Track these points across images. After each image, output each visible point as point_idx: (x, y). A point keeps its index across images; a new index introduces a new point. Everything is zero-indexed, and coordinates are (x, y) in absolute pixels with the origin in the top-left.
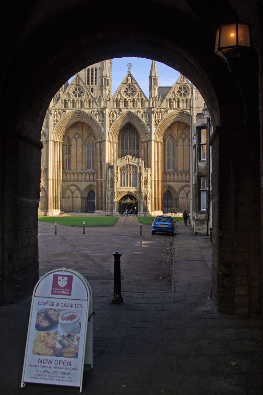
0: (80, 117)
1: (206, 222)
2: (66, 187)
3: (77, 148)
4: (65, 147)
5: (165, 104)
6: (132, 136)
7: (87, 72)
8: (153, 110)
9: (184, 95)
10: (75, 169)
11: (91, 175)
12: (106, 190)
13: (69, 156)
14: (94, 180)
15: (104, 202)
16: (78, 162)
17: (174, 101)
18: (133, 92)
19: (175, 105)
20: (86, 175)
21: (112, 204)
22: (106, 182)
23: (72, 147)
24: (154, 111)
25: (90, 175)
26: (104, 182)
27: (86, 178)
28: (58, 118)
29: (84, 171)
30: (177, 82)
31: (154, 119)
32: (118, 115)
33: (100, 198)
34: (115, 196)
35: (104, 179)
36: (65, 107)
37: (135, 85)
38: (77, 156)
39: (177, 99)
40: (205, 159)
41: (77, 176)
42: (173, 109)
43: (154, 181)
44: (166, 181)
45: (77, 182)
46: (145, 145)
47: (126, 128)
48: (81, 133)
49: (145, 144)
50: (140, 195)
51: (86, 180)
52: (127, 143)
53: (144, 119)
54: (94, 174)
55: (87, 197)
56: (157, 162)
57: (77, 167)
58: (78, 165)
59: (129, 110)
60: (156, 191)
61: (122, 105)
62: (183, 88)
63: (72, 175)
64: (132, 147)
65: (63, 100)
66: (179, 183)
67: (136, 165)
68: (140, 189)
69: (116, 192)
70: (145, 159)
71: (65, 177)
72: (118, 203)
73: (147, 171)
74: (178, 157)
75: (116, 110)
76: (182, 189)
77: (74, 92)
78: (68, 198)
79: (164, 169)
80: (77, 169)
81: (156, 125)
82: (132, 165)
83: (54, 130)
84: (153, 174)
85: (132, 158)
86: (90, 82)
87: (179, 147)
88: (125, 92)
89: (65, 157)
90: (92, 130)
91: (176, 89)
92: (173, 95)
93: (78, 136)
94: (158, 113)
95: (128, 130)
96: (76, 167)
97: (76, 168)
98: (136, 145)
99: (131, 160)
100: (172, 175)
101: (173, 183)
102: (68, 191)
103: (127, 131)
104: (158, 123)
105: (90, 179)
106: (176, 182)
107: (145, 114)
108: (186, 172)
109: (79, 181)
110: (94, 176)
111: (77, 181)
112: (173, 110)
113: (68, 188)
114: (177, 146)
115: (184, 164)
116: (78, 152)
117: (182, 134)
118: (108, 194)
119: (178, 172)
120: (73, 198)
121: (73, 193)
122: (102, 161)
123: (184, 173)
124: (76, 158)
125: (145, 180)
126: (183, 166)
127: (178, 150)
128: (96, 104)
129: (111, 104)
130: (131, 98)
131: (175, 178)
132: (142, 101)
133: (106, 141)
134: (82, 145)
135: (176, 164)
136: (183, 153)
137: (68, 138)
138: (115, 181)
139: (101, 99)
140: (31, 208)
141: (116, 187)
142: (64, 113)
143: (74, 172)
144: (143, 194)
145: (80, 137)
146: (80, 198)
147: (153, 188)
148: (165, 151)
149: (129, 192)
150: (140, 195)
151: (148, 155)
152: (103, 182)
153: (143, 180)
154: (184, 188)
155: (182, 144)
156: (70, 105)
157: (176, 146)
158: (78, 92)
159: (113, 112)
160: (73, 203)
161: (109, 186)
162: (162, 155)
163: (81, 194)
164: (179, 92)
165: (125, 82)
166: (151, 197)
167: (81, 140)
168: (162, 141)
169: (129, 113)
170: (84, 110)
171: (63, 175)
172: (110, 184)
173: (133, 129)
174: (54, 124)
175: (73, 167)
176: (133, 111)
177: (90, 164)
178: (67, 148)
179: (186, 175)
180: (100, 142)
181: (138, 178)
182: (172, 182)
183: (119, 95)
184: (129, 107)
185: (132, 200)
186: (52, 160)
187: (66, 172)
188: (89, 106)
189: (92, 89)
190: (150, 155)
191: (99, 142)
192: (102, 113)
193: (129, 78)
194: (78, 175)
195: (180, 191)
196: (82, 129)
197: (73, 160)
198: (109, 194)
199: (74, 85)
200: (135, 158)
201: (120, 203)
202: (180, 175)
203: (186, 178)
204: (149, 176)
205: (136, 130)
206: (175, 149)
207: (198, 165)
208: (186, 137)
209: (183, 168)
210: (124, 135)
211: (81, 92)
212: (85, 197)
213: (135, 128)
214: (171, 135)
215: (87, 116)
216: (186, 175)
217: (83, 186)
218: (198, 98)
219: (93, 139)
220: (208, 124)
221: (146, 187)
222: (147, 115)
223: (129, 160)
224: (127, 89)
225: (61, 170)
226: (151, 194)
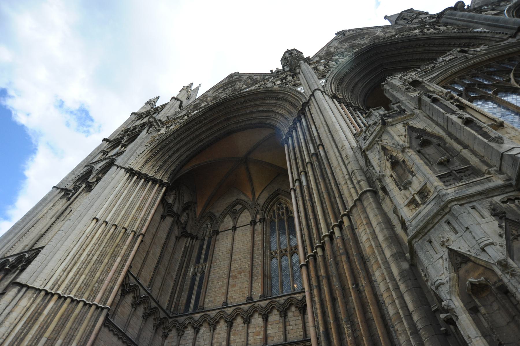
11: (290, 314)
16: (235, 277)
20: (266, 319)
25: (284, 314)
27: (266, 337)
41: (225, 335)
48: (251, 197)
54: (303, 309)
58: (235, 286)
105: (285, 335)
116: (236, 246)
167: (248, 214)
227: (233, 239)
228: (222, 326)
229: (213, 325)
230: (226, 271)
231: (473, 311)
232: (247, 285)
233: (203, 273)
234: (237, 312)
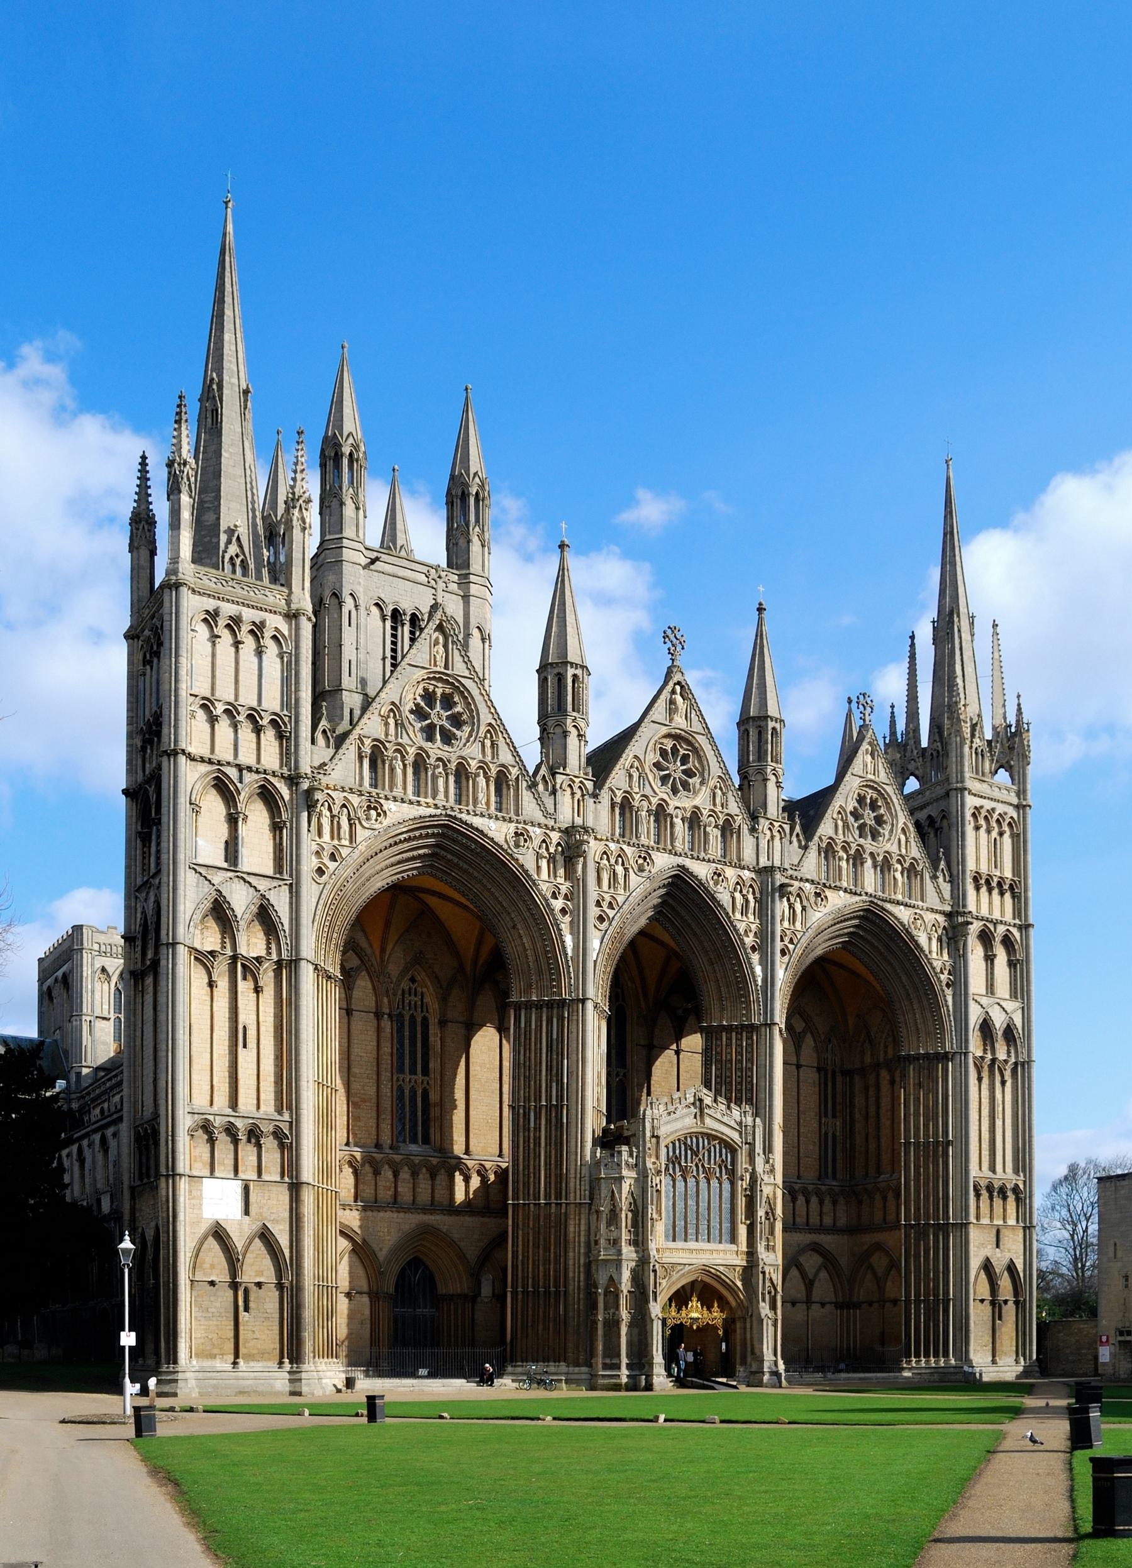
5: (812, 864)
7: (389, 623)
8: (779, 879)
9: (875, 835)
18: (689, 773)
24: (782, 886)
28: (339, 839)
29: (388, 1151)
42: (845, 891)
46: (729, 1045)
49: (729, 1039)
53: (738, 916)
59: (680, 860)
62: (868, 801)
65: (368, 742)
68: (751, 1254)
75: (625, 847)
82: (715, 1138)
83: (321, 902)
88: (657, 765)
91: (849, 799)
94: (792, 899)
104: (791, 947)
107: (745, 892)
112: (841, 893)
115: (802, 1151)
118: (611, 1279)
122: (559, 1108)
128: (538, 799)
132: (727, 829)
139: (559, 779)
149: (706, 1270)
152: (566, 1213)
153: (761, 1213)
156: (404, 778)
159: (613, 861)
164: (856, 815)
174: (320, 871)
176: (701, 870)
180: (550, 1005)
181: (741, 1202)
183: (636, 775)
184: (678, 845)
185: (709, 1308)
191: (539, 1006)
192: (570, 851)
216: (808, 1202)
222: (750, 897)
223: (701, 1110)
224: (663, 753)
231: (605, 1295)
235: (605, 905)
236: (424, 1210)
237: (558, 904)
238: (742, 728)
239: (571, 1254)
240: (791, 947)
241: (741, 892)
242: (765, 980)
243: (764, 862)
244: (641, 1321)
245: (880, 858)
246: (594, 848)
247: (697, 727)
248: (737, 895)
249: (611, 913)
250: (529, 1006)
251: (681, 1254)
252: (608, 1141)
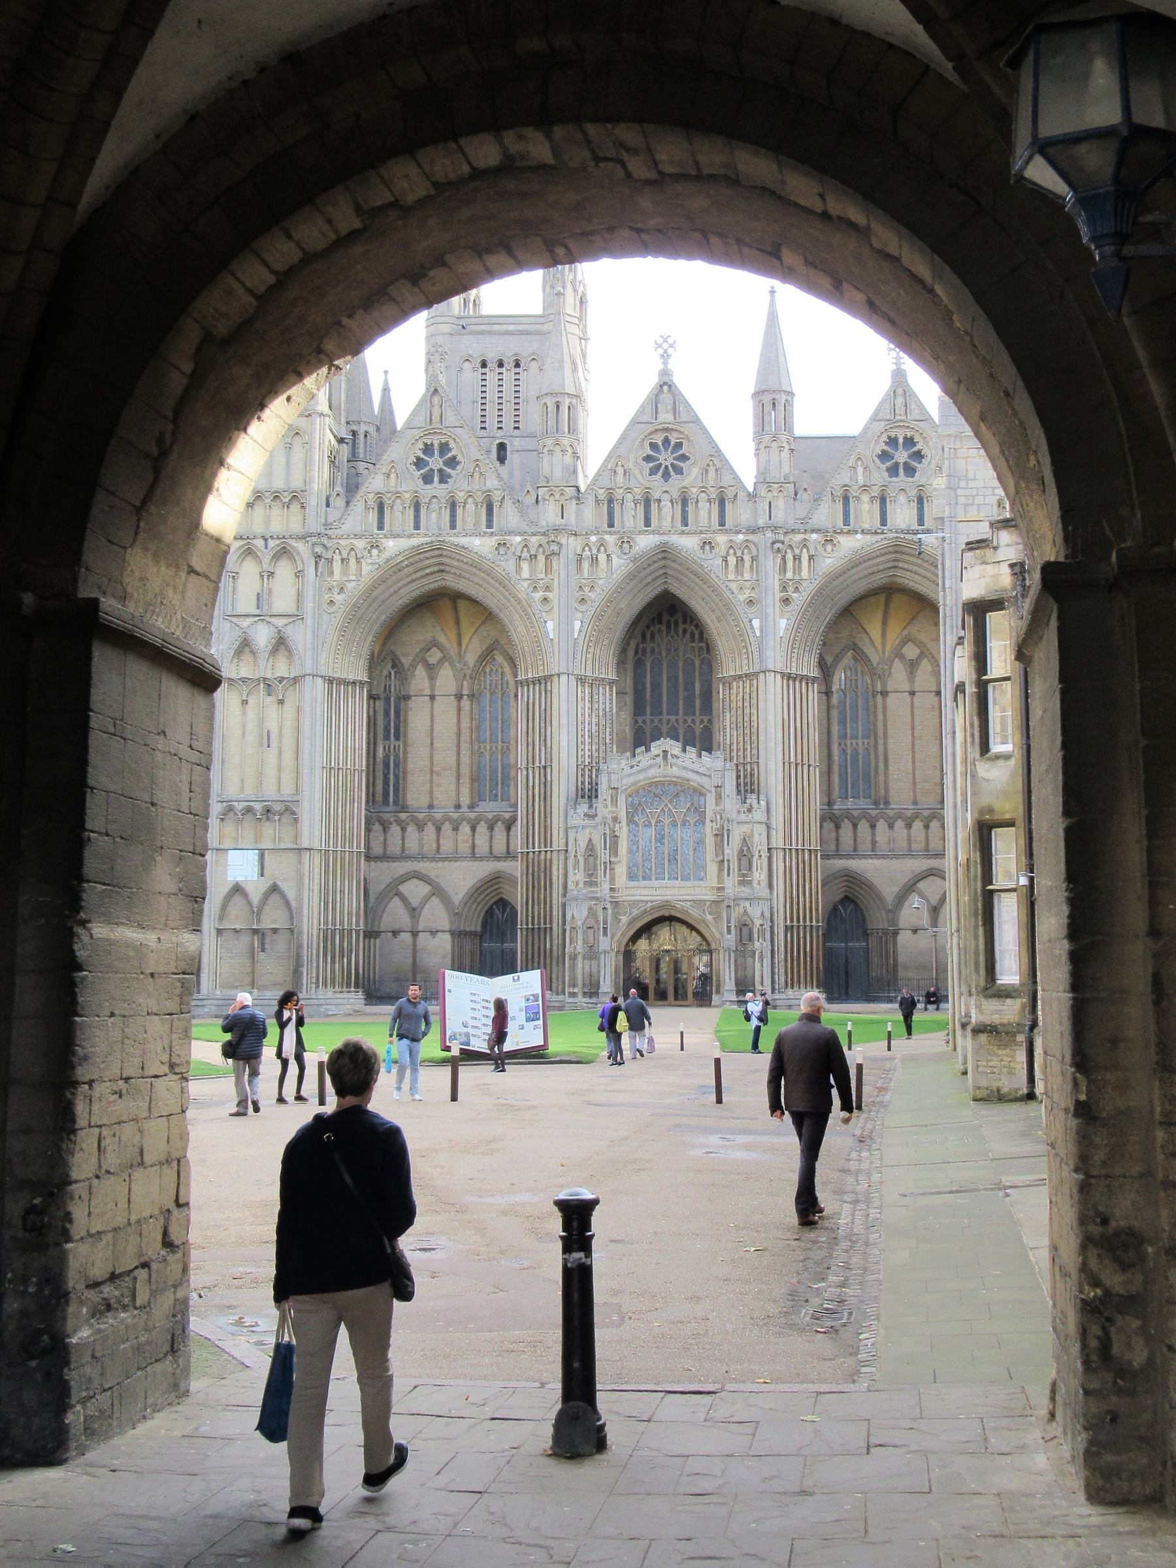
0: (449, 572)
1: (1021, 1038)
2: (382, 887)
3: (436, 708)
4: (380, 705)
5: (827, 514)
6: (681, 654)
10: (426, 804)
11: (496, 829)
12: (564, 895)
13: (397, 743)
14: (509, 855)
15: (555, 954)
16: (438, 774)
17: (865, 498)
18: (684, 458)
19: (866, 512)
20: (473, 829)
21: (594, 963)
22: (566, 859)
23: (411, 704)
25: (491, 828)
26: (555, 862)
27: (473, 847)
30: (876, 413)
31: (777, 577)
32: (616, 561)
33: (539, 932)
34: (605, 922)
35: (555, 847)
36: (380, 528)
37: (687, 429)
38: (432, 744)
39: (875, 491)
40: (1008, 748)
41: (433, 837)
43: (781, 854)
44: (837, 854)
45: (433, 864)
46: (737, 694)
47: (653, 620)
50: (717, 918)
51: (473, 853)
52: (656, 686)
53: (731, 576)
54: (509, 825)
55: (479, 929)
56: (793, 766)
57: (436, 794)
58: (440, 785)
59: (666, 538)
60: (792, 898)
61: (630, 517)
62: (901, 441)
63: (411, 829)
64: (681, 702)
66: (894, 862)
67: (704, 781)
69: (609, 906)
70: (741, 753)
71: (382, 838)
72: (621, 958)
73: (749, 810)
74: (890, 746)
76: (910, 888)
77: (419, 463)
78: (395, 933)
79: (826, 800)
80: (435, 803)
81: (786, 601)
84: (778, 820)
85: (684, 750)
86: (492, 423)
87: (891, 699)
88: (648, 459)
89: (381, 750)
90: (503, 630)
92: (860, 470)
93: (439, 655)
95: (664, 628)
96: (431, 792)
97: (432, 798)
98: (697, 692)
99: (679, 762)
100: (864, 827)
101: (870, 861)
102: (391, 905)
103: (660, 631)
105: (491, 847)
106: (885, 857)
107: (739, 554)
108: (926, 813)
109: (445, 859)
110: (511, 833)
111: (433, 859)
113: (394, 889)
114: (884, 694)
115: (917, 776)
116: (437, 728)
117: (904, 643)
119: (891, 813)
120: (415, 934)
121: (417, 912)
122: (545, 767)
123: (916, 816)
124: (432, 756)
125: (741, 850)
126: (914, 784)
127: (889, 714)
129: (591, 515)
130: (676, 482)
131: (877, 839)
133: (564, 678)
134: (459, 697)
135: (881, 778)
136: (913, 728)
137: (393, 667)
138: (603, 855)
139: (541, 492)
140: (152, 975)
141: (612, 880)
142: (375, 552)
143: (420, 816)
144: (734, 915)
145: (446, 658)
146: (447, 937)
147: (779, 884)
148: (829, 719)
149: (666, 904)
150: (717, 918)
151: (754, 738)
154: (920, 885)
155: (907, 687)
157: (879, 697)
158: (436, 463)
160: (414, 958)
161: (577, 876)
162: (815, 736)
163: (455, 915)
164: (884, 456)
165: (646, 418)
166: (772, 927)
168: (814, 672)
169: (664, 553)
170: (464, 541)
171: (368, 830)
172: (582, 868)
173: (685, 622)
175: (416, 796)
176: (688, 543)
177: (490, 779)
178: (387, 713)
179: (927, 827)
181: (710, 841)
182: (864, 857)
183: (620, 470)
186: (318, 766)
187: (386, 816)
188: (490, 526)
189: (502, 447)
190: (761, 738)
193: (666, 397)
194: (438, 829)
195: (902, 898)
196: (458, 623)
197: (417, 760)
198: (578, 913)
199: (417, 433)
200: (693, 750)
201: (628, 956)
202: (899, 824)
203: (927, 838)
204: (763, 828)
205: (697, 626)
206: (875, 706)
207: (974, 776)
208: (922, 655)
209: (914, 792)
210: (644, 651)
211: (453, 462)
212: (473, 928)
213: (692, 620)
214: (855, 647)
215: (477, 565)
216: (927, 827)
217: (461, 878)
218: (971, 476)
219: (507, 670)
220: (1014, 588)
221: (744, 882)
224: (653, 446)
225: (360, 809)
226: (772, 915)
227: (432, 715)
228: (430, 829)
229: (421, 827)
230: (427, 763)
232: (453, 788)
233: (397, 756)
234: (447, 819)
235: (587, 589)
236: (498, 859)
237: (538, 595)
238: (758, 398)
239: (555, 895)
240: (795, 595)
241: (735, 554)
242: (761, 631)
243: (761, 522)
244: (592, 954)
245: (914, 493)
246: (572, 545)
247: (684, 417)
248: (732, 560)
249: (592, 595)
250: (527, 683)
251: (643, 892)
252: (588, 793)
